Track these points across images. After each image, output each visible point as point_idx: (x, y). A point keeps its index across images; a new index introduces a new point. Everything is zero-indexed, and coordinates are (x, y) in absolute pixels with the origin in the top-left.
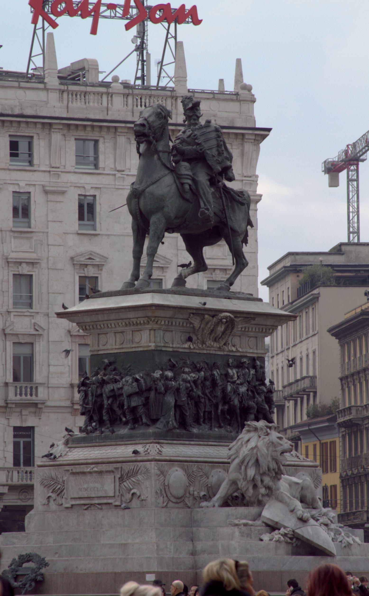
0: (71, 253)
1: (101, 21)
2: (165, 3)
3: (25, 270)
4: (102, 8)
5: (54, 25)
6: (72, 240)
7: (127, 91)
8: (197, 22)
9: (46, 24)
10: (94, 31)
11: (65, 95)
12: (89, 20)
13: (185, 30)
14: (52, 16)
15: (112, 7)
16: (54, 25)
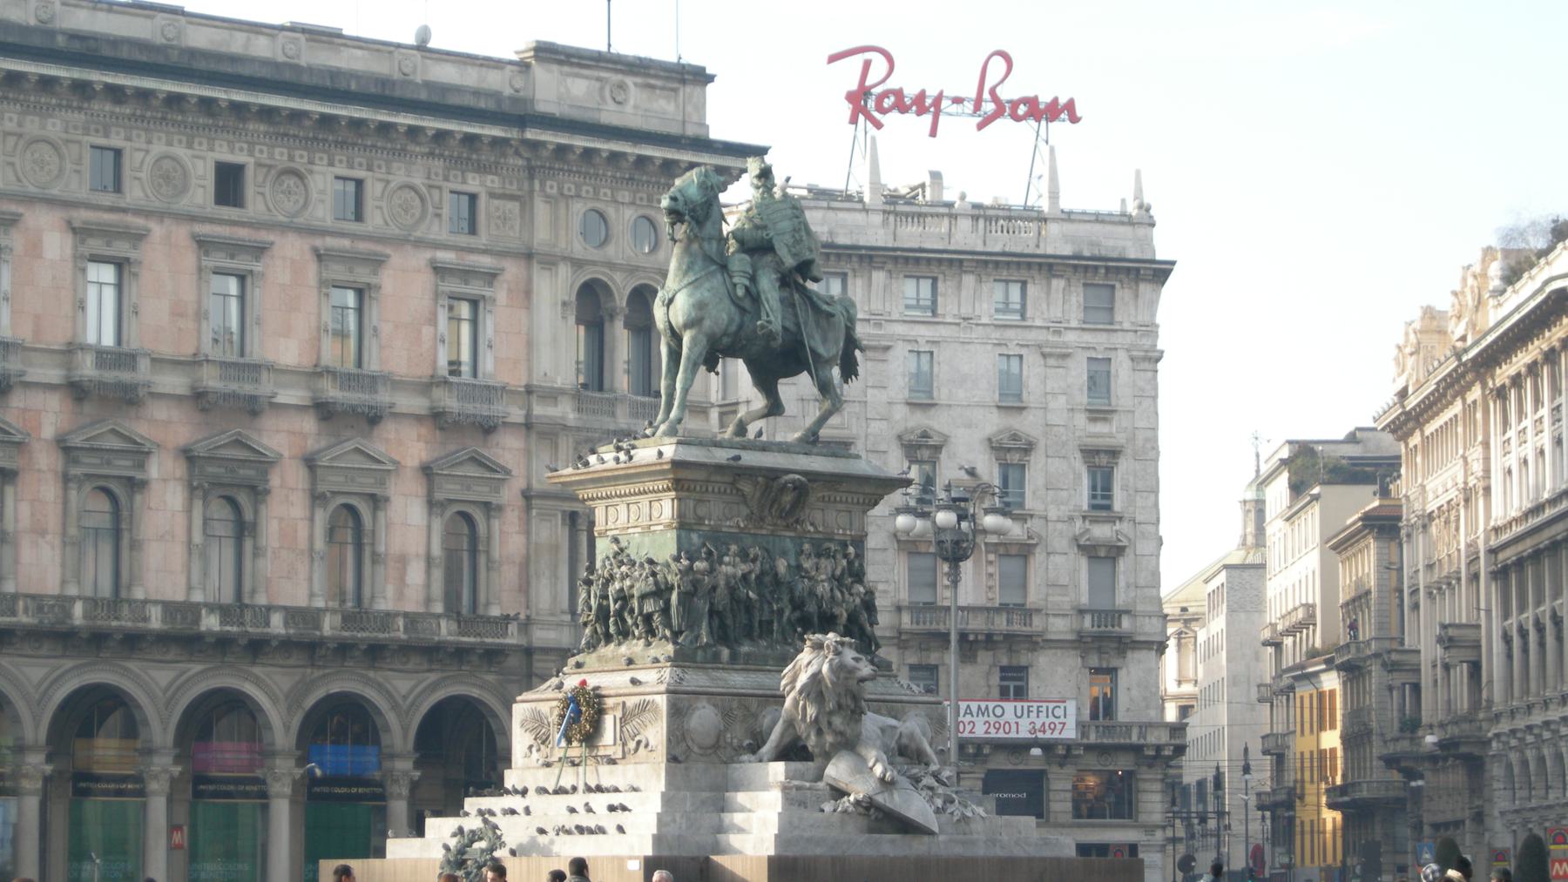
0: (899, 428)
1: (942, 118)
2: (1031, 94)
4: (945, 104)
5: (878, 125)
6: (900, 412)
7: (976, 212)
8: (1074, 119)
9: (869, 124)
10: (933, 133)
12: (927, 119)
13: (1060, 129)
14: (876, 115)
15: (958, 101)
16: (878, 125)
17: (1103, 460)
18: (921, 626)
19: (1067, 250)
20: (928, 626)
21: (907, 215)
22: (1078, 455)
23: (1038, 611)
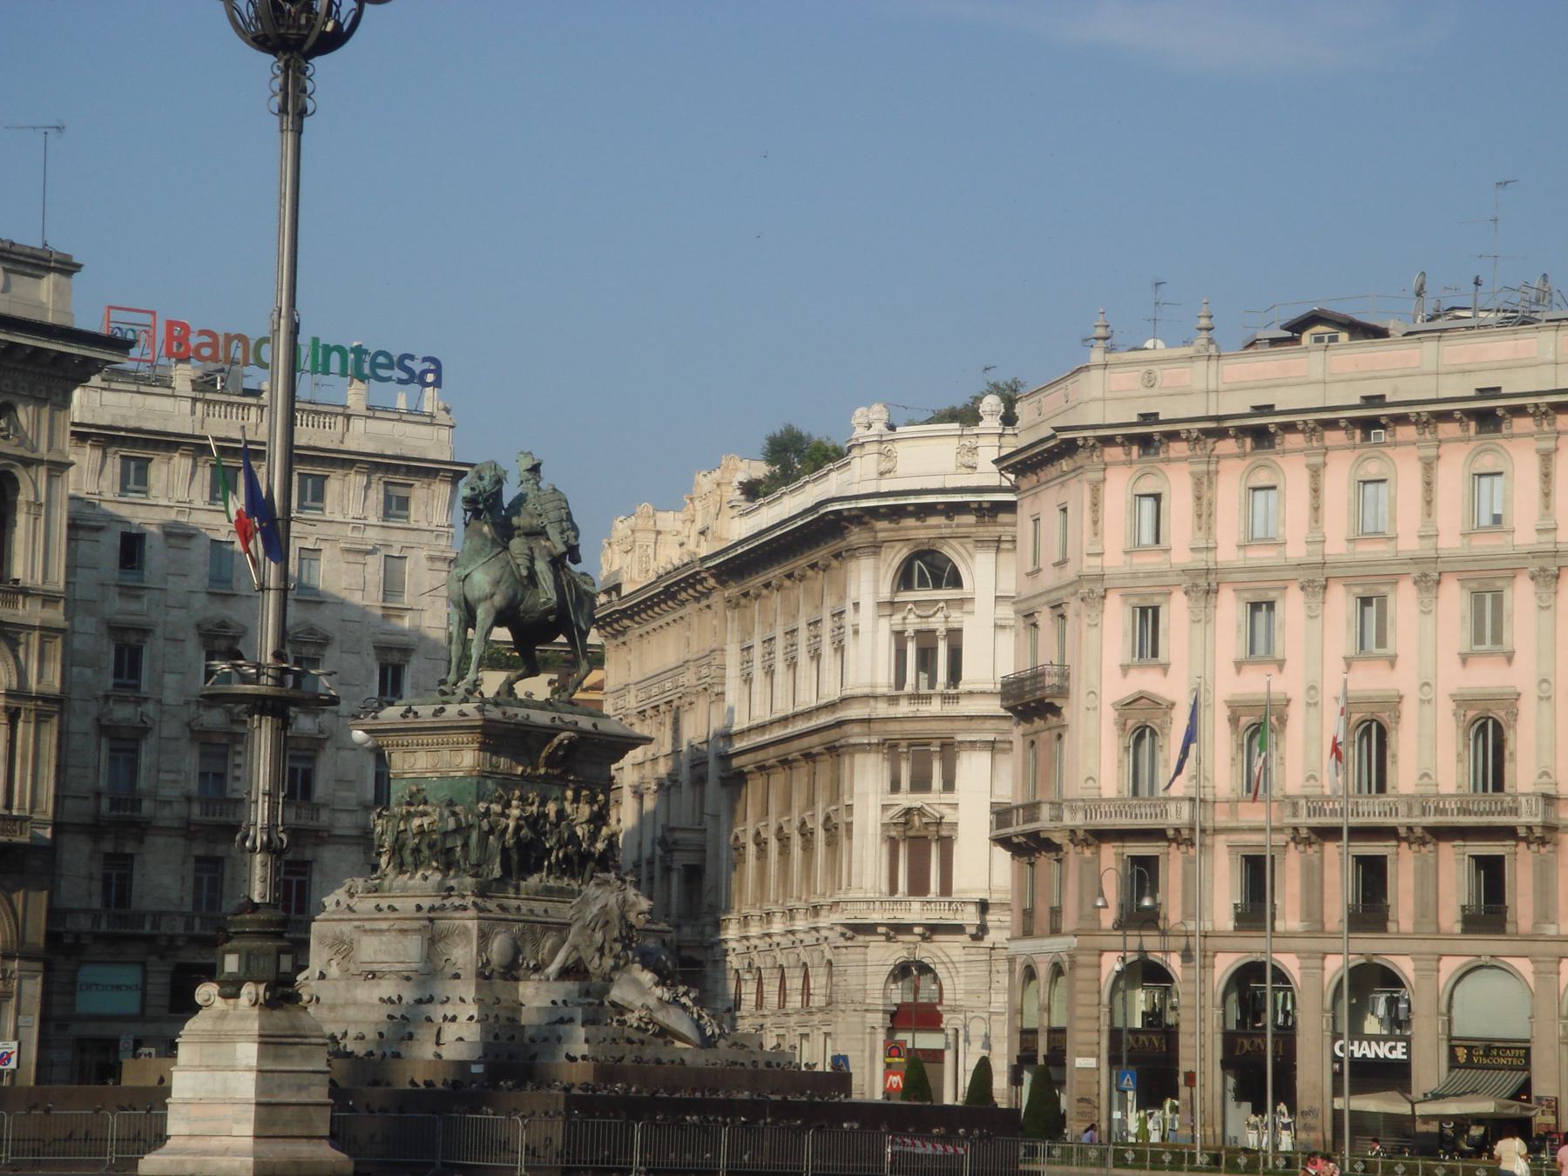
3: (133, 639)
6: (200, 601)
11: (199, 405)
17: (395, 658)
18: (211, 818)
19: (370, 448)
20: (217, 818)
21: (216, 402)
22: (372, 652)
23: (325, 805)
